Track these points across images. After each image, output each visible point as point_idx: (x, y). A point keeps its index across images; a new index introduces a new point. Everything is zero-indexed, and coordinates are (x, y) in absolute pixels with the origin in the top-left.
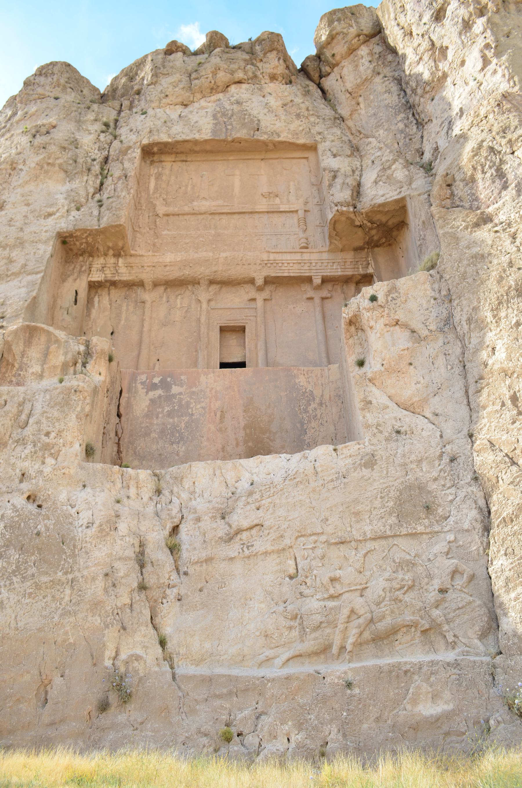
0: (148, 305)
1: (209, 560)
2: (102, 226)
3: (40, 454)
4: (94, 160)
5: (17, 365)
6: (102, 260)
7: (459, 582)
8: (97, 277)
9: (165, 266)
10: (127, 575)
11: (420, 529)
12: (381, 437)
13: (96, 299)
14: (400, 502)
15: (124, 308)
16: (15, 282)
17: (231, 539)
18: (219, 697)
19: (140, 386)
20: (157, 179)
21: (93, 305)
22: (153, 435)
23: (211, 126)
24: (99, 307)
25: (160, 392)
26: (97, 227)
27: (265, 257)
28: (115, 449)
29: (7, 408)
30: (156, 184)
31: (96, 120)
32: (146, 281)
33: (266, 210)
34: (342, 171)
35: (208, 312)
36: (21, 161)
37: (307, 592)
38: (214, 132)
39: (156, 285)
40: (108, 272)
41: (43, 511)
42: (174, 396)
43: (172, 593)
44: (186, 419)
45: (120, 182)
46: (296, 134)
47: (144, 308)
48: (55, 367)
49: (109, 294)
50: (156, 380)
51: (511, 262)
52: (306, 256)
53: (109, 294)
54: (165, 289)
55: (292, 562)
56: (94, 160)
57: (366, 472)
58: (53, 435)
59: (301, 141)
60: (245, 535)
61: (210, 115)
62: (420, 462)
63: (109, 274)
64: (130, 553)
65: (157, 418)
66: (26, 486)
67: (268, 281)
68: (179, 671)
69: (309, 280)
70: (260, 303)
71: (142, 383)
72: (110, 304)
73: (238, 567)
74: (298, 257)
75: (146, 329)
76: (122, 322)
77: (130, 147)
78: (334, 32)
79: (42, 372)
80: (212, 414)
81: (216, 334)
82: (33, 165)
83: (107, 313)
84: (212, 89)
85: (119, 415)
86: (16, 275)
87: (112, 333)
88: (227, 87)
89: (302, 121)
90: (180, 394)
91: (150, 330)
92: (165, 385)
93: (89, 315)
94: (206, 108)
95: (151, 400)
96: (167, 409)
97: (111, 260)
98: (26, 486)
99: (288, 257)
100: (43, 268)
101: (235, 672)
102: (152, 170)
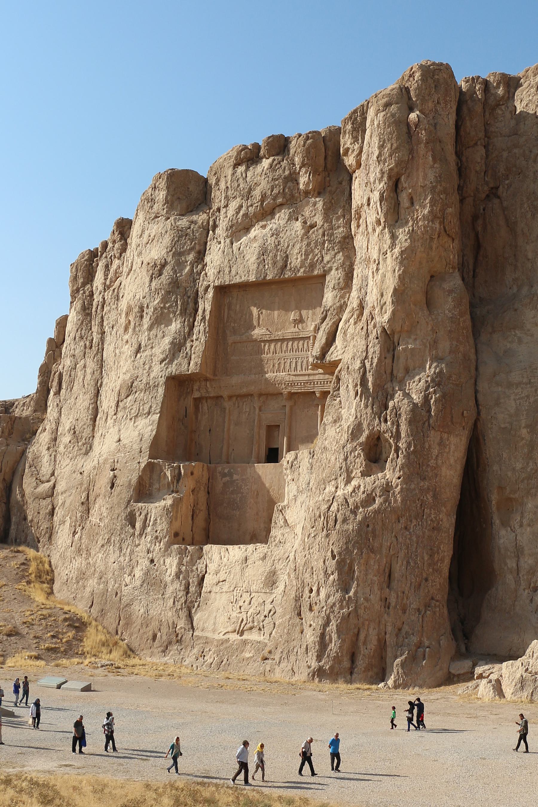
0: (227, 411)
1: (210, 592)
2: (190, 372)
3: (154, 541)
4: (189, 297)
5: (147, 486)
6: (198, 384)
7: (272, 613)
8: (197, 395)
9: (233, 386)
10: (181, 597)
11: (268, 591)
12: (274, 544)
13: (200, 406)
14: (266, 578)
15: (215, 412)
16: (147, 421)
17: (217, 585)
18: (203, 643)
19: (218, 475)
20: (229, 309)
21: (199, 410)
22: (225, 505)
23: (256, 265)
24: (202, 411)
25: (228, 478)
26: (187, 373)
27: (287, 378)
28: (207, 513)
29: (141, 516)
30: (228, 314)
31: (192, 249)
32: (224, 396)
33: (291, 337)
34: (332, 309)
35: (259, 415)
36: (146, 306)
37: (234, 609)
38: (257, 274)
39: (230, 397)
40: (201, 391)
41: (156, 568)
42: (235, 481)
43: (196, 605)
44: (240, 495)
45: (202, 325)
46: (312, 266)
47: (225, 412)
48: (165, 485)
49: (207, 402)
50: (226, 471)
51: (329, 460)
52: (311, 378)
53: (207, 402)
54: (236, 399)
55: (232, 597)
56: (189, 297)
57: (261, 562)
58: (158, 532)
59: (316, 273)
60: (221, 583)
61: (257, 250)
62: (279, 560)
63: (203, 391)
64: (182, 588)
65: (227, 494)
66: (150, 555)
67: (292, 395)
68: (194, 634)
69: (314, 392)
70: (287, 409)
71: (220, 473)
72: (208, 409)
73: (218, 596)
74: (306, 378)
75: (226, 429)
76: (215, 422)
77: (209, 286)
78: (346, 147)
79: (159, 487)
80: (253, 493)
81: (263, 433)
82: (152, 310)
83: (207, 416)
84: (263, 214)
85: (208, 493)
86: (149, 413)
87: (210, 430)
88: (274, 209)
89: (318, 249)
90: (237, 480)
91: (229, 429)
92: (230, 474)
93: (197, 418)
94: (256, 240)
95: (224, 483)
96: (231, 489)
97: (203, 383)
98: (150, 555)
99: (301, 378)
100: (159, 410)
101: (209, 635)
102: (226, 300)
